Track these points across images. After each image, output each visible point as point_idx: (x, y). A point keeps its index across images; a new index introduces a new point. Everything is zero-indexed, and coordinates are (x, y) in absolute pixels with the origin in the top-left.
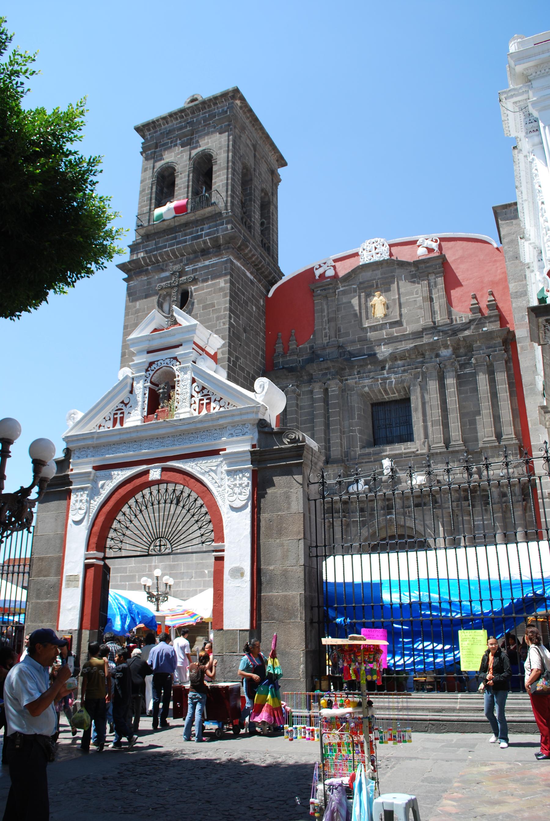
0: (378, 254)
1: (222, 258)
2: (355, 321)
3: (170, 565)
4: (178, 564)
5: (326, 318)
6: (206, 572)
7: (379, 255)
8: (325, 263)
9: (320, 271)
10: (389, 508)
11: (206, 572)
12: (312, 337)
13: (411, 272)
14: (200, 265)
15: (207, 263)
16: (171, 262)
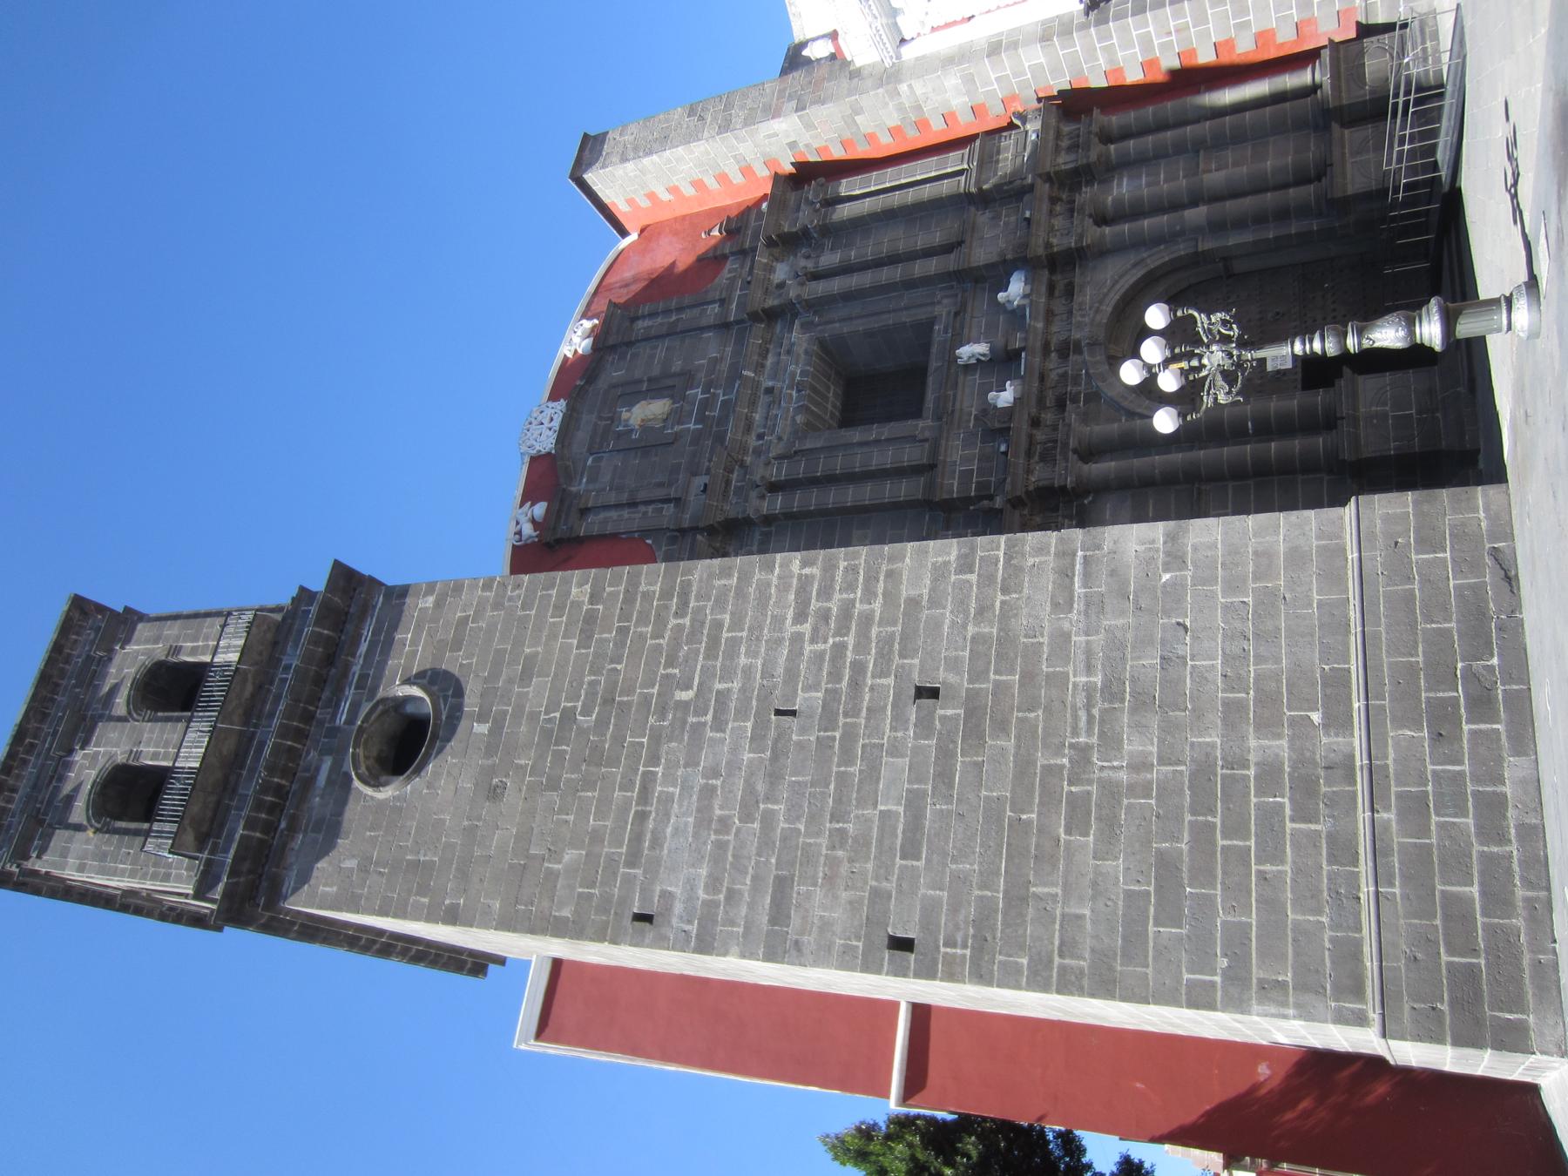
0: (552, 419)
1: (375, 607)
2: (656, 455)
3: (1134, 710)
4: (1134, 680)
5: (625, 513)
6: (1166, 577)
7: (555, 417)
8: (518, 523)
9: (528, 530)
10: (1067, 349)
11: (1166, 577)
12: (649, 541)
13: (613, 363)
14: (357, 669)
15: (363, 648)
16: (308, 753)
